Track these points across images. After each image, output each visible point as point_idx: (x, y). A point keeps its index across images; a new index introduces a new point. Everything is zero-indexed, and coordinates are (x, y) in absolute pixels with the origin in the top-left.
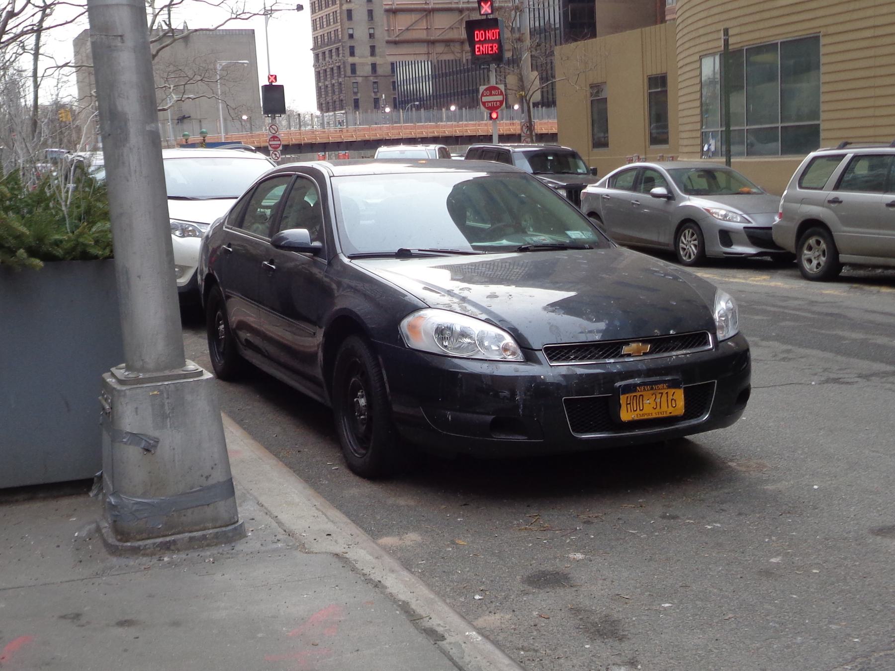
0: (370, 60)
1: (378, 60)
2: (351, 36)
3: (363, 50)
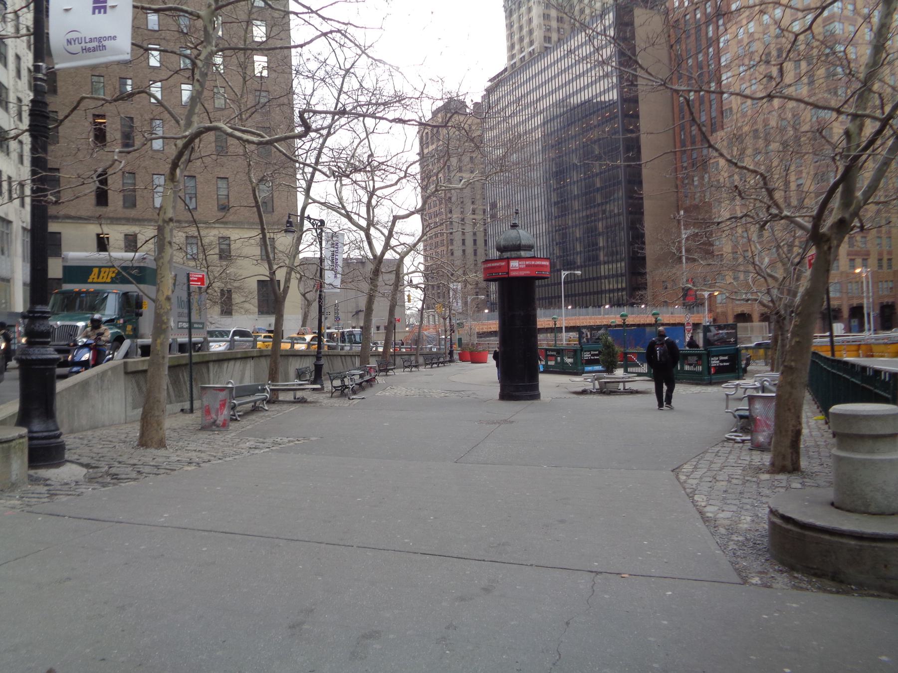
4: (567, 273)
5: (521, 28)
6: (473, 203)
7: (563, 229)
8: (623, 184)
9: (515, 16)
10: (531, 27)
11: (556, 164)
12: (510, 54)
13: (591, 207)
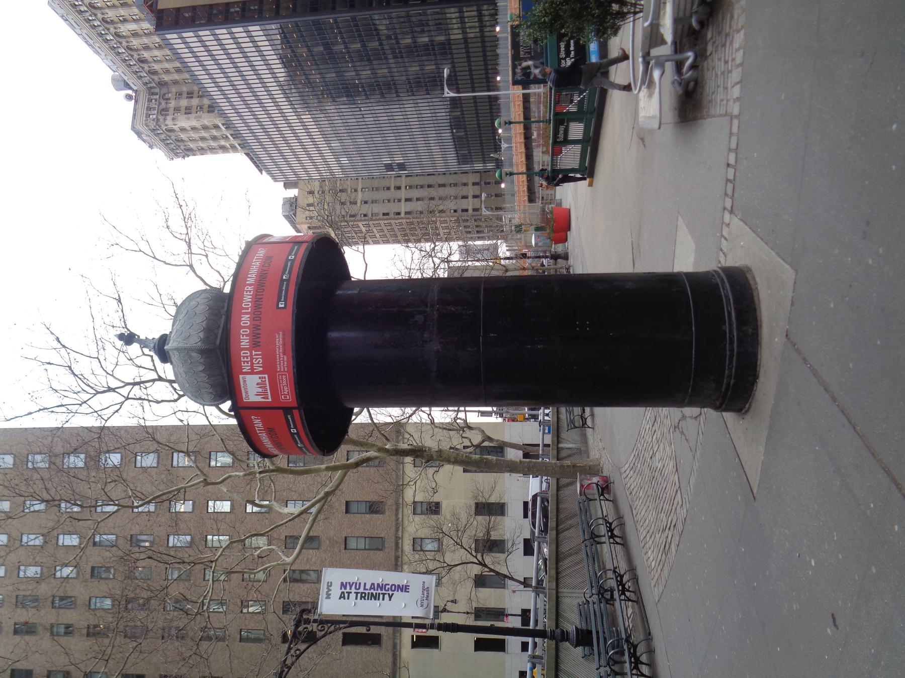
0: (470, 199)
1: (471, 194)
2: (455, 211)
3: (464, 204)
4: (446, 89)
5: (203, 139)
6: (388, 189)
7: (411, 87)
8: (355, 14)
9: (192, 145)
10: (200, 127)
11: (339, 97)
12: (231, 150)
13: (384, 54)
